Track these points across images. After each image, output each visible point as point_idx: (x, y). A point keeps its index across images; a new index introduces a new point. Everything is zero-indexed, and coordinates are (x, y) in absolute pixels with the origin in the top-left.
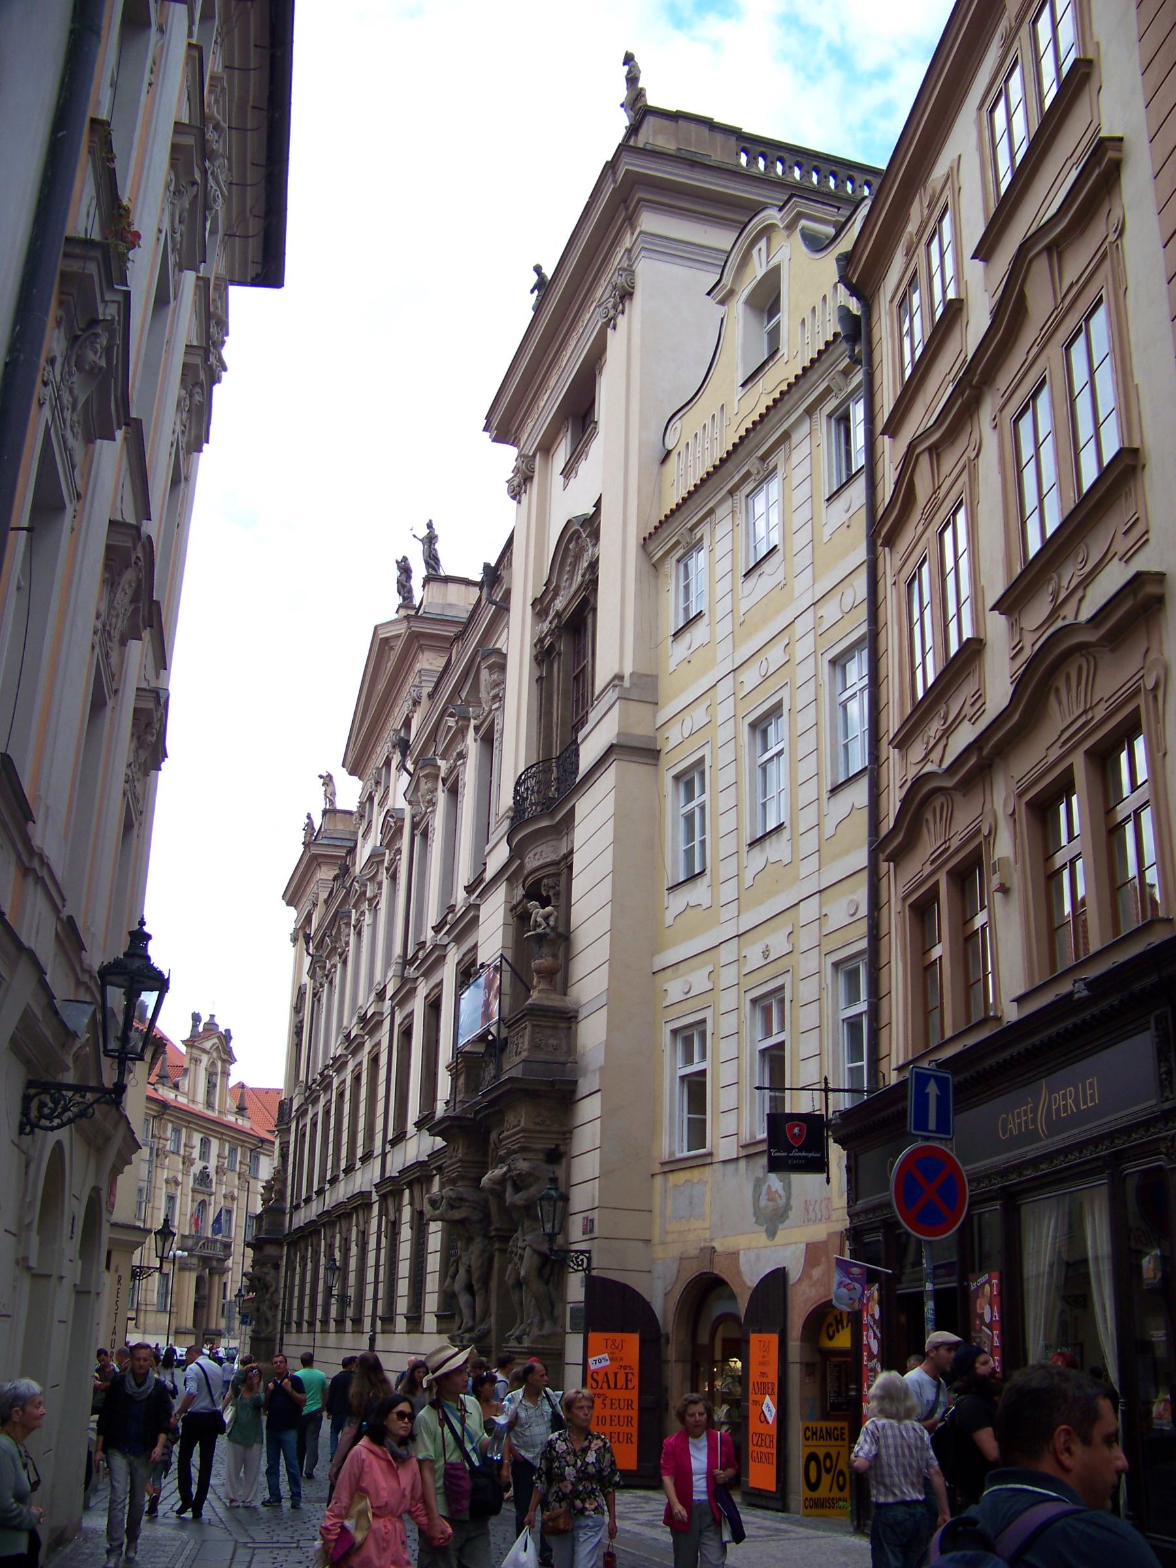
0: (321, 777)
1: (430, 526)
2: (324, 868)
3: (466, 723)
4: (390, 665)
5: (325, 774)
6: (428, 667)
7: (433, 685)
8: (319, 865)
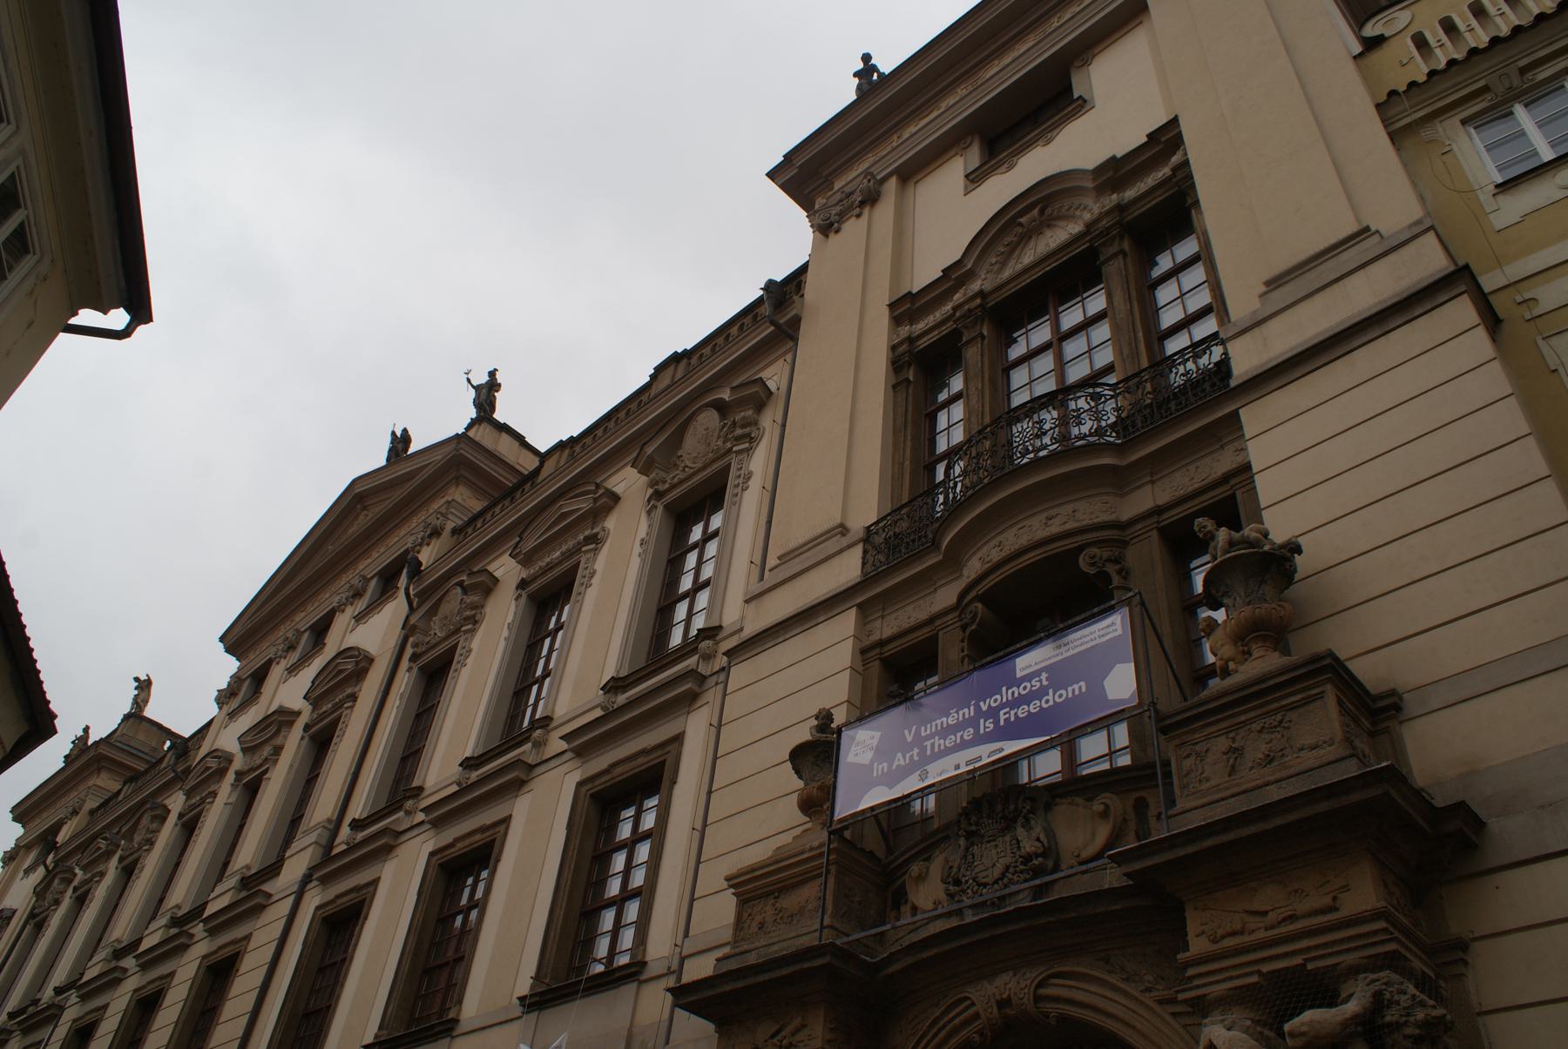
0: (137, 679)
1: (492, 374)
2: (104, 775)
3: (611, 503)
5: (143, 678)
8: (99, 770)
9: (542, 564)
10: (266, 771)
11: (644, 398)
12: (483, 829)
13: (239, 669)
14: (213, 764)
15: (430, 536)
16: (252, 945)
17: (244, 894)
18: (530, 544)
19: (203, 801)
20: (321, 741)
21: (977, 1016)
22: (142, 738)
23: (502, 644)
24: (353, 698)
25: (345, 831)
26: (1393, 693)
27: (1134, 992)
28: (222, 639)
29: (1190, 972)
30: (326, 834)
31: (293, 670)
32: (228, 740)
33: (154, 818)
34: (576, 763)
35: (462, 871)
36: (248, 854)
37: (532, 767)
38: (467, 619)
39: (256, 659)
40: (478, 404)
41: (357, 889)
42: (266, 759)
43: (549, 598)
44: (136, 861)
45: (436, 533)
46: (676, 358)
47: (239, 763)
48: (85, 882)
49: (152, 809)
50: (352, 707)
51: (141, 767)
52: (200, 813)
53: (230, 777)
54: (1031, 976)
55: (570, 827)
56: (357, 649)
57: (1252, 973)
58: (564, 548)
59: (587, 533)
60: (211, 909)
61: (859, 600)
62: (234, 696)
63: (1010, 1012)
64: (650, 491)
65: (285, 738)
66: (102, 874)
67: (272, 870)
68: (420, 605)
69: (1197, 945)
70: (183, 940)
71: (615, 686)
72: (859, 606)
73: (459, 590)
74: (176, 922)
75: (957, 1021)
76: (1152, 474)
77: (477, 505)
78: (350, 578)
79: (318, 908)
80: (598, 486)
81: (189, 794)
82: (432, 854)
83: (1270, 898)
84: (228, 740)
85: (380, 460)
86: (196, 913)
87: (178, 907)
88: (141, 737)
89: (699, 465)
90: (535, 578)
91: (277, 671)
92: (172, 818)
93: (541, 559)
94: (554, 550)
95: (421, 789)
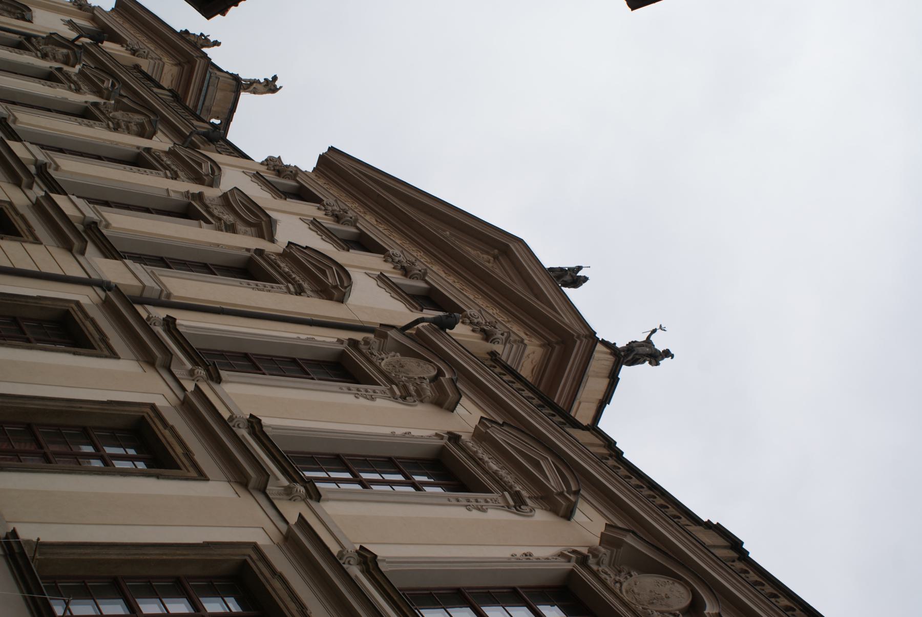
1: (667, 354)
2: (175, 70)
3: (561, 512)
4: (473, 253)
5: (278, 84)
6: (527, 352)
7: (504, 358)
8: (179, 64)
9: (481, 453)
10: (208, 222)
11: (684, 520)
12: (188, 454)
13: (305, 173)
14: (206, 168)
15: (483, 331)
16: (28, 246)
17: (80, 228)
18: (498, 435)
19: (166, 167)
20: (248, 269)
22: (219, 96)
23: (387, 431)
24: (300, 291)
25: (161, 313)
28: (331, 149)
30: (155, 295)
31: (315, 225)
32: (233, 178)
33: (141, 125)
34: (277, 538)
35: (144, 442)
36: (120, 223)
37: (263, 491)
38: (405, 387)
39: (318, 187)
40: (632, 346)
41: (104, 338)
42: (220, 219)
43: (445, 469)
44: (96, 119)
45: (487, 336)
46: (735, 544)
47: (211, 193)
48: (68, 77)
49: (150, 121)
50: (290, 292)
51: (190, 102)
52: (154, 168)
53: (195, 188)
55: (207, 545)
56: (350, 284)
58: (503, 473)
59: (524, 494)
60: (59, 199)
62: (277, 175)
64: (585, 551)
65: (245, 233)
66: (78, 90)
67: (109, 250)
68: (409, 337)
70: (25, 180)
71: (367, 560)
73: (434, 373)
74: (42, 169)
77: (526, 371)
78: (421, 260)
79: (77, 303)
80: (577, 493)
81: (171, 153)
82: (153, 407)
84: (233, 178)
85: (548, 262)
86: (54, 186)
87: (57, 168)
88: (219, 95)
89: (626, 597)
90: (464, 449)
91: (310, 210)
92: (144, 143)
93: (485, 451)
94: (498, 462)
95: (219, 380)
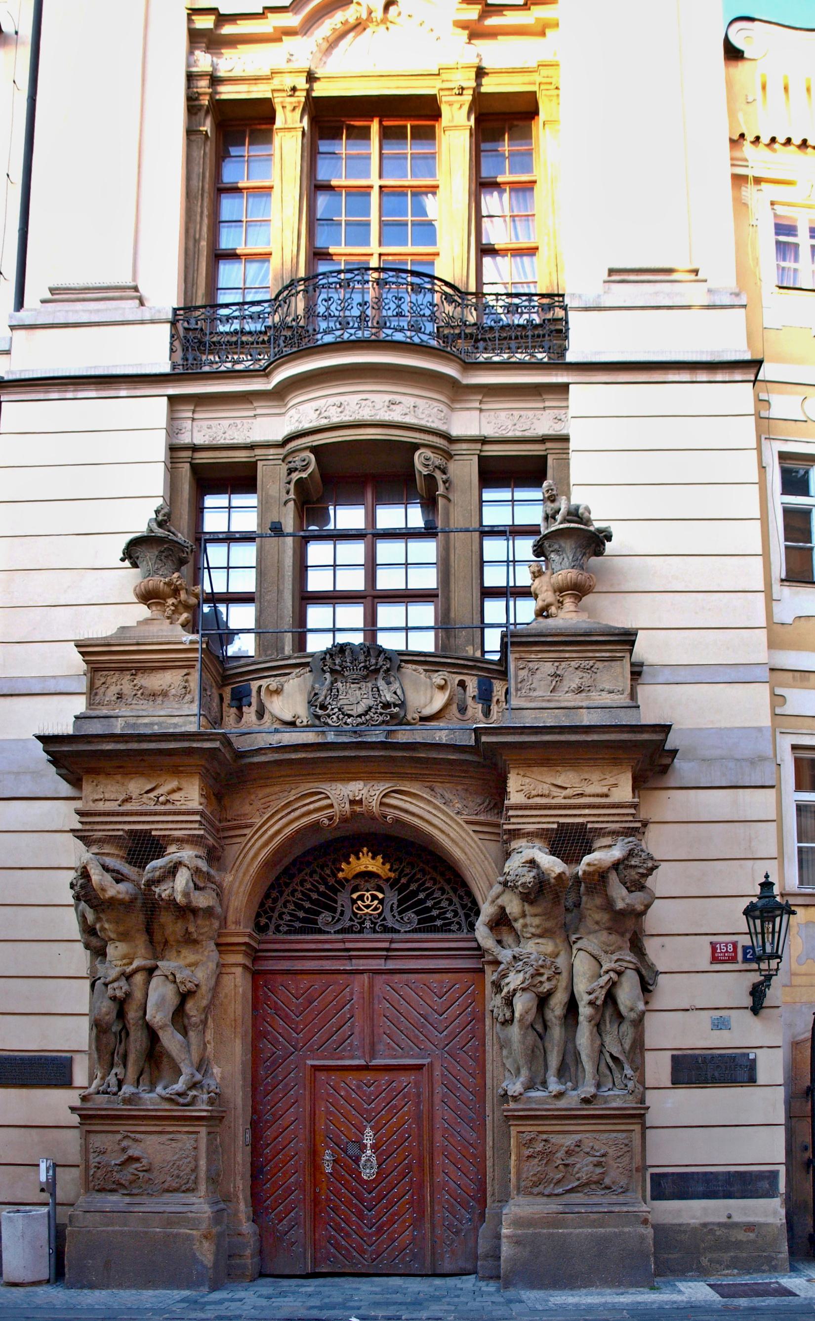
21: (331, 806)
26: (641, 665)
27: (452, 814)
29: (511, 813)
54: (382, 787)
57: (553, 823)
61: (171, 391)
63: (358, 809)
69: (515, 797)
72: (172, 399)
75: (312, 807)
76: (481, 402)
83: (568, 778)
